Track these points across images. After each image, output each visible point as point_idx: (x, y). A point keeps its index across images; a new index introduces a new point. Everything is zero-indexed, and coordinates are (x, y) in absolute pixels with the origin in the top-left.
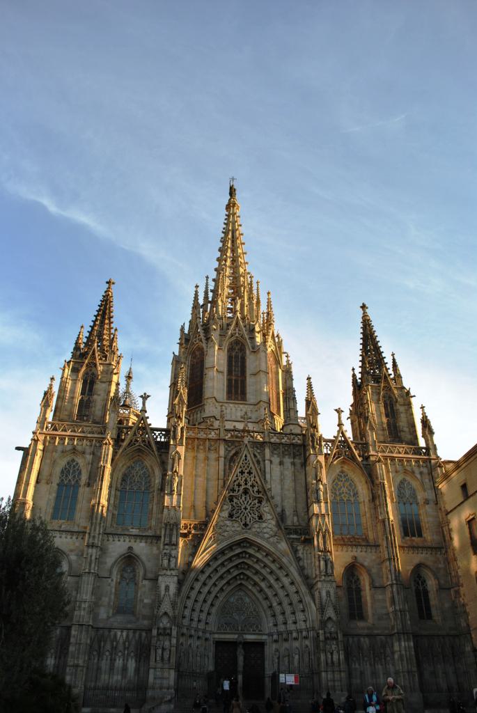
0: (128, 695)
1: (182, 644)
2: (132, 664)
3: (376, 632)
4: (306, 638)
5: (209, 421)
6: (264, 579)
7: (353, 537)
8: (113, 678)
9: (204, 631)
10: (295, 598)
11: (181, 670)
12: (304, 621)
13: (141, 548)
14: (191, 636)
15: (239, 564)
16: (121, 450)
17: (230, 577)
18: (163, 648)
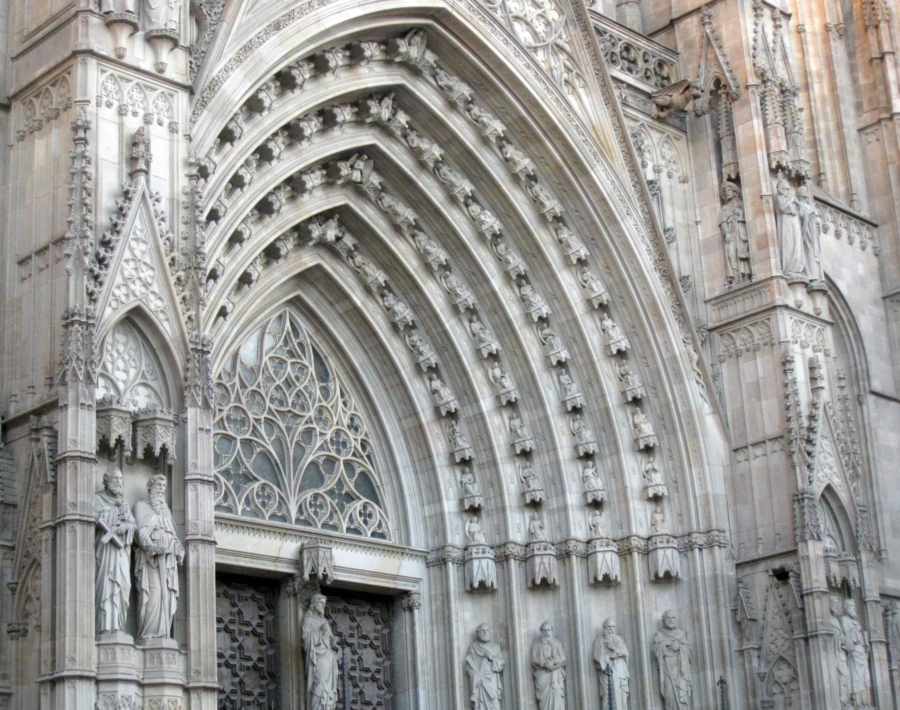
4: (667, 580)
18: (136, 546)
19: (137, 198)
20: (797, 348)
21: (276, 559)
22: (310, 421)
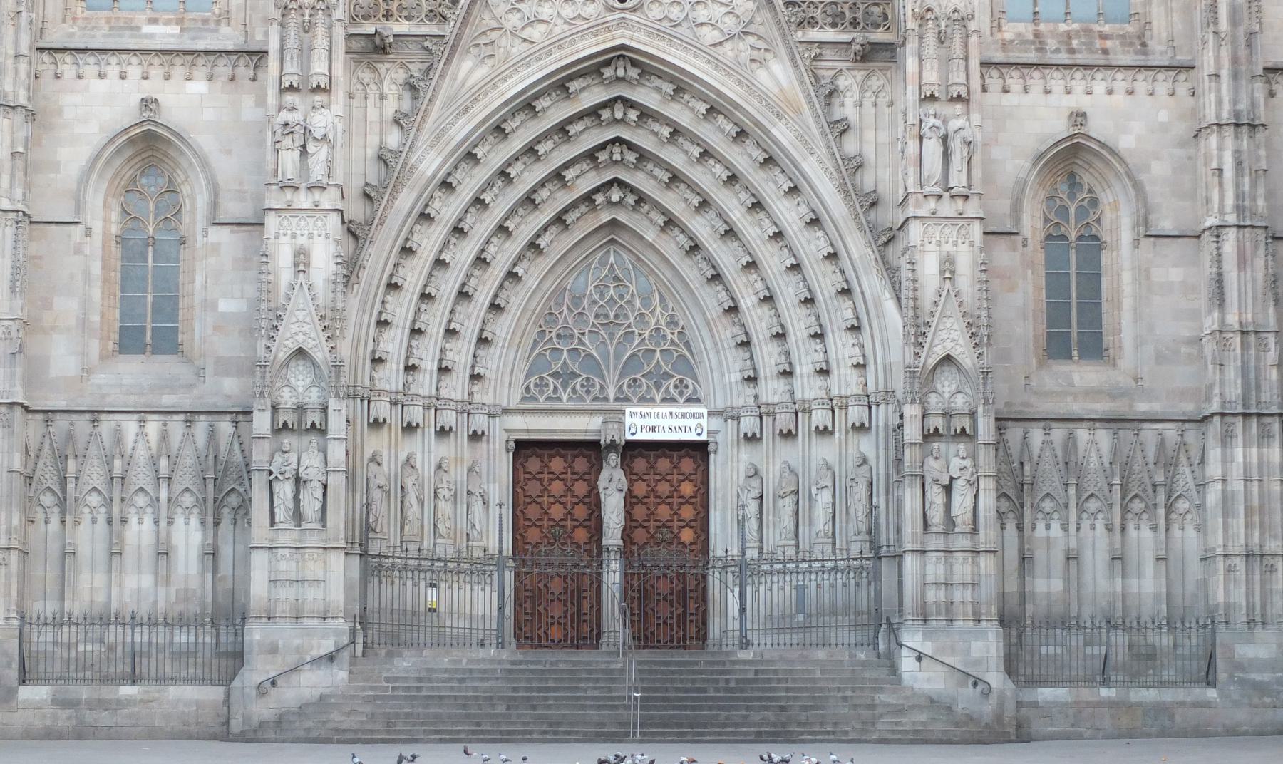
0: (183, 637)
1: (374, 459)
2: (188, 536)
3: (1142, 407)
4: (861, 428)
6: (705, 204)
7: (1088, 32)
8: (120, 586)
9: (465, 410)
10: (825, 281)
11: (374, 548)
12: (860, 366)
13: (190, 101)
14: (410, 428)
15: (602, 147)
17: (564, 198)
19: (297, 287)
20: (932, 247)
21: (586, 431)
22: (629, 326)
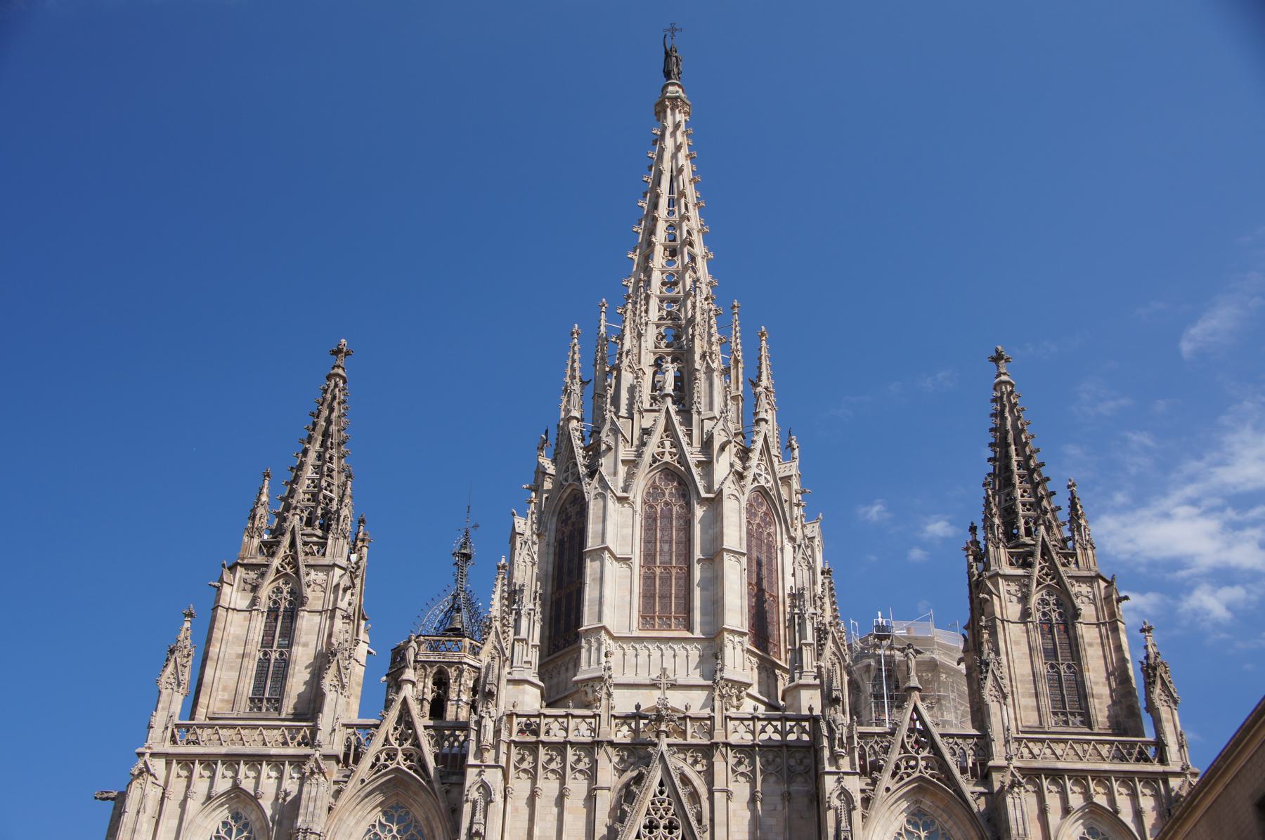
5: (589, 691)
16: (350, 784)
